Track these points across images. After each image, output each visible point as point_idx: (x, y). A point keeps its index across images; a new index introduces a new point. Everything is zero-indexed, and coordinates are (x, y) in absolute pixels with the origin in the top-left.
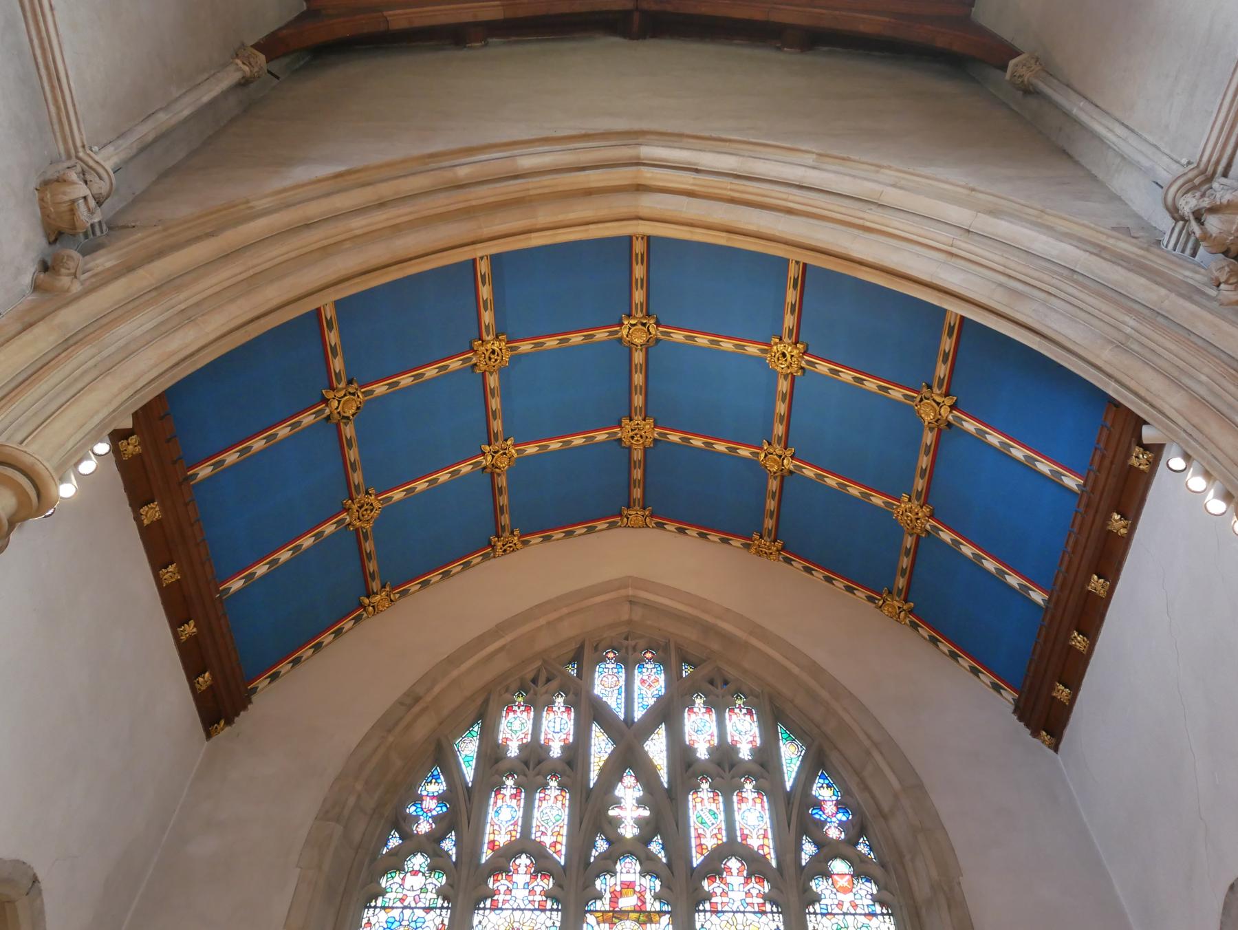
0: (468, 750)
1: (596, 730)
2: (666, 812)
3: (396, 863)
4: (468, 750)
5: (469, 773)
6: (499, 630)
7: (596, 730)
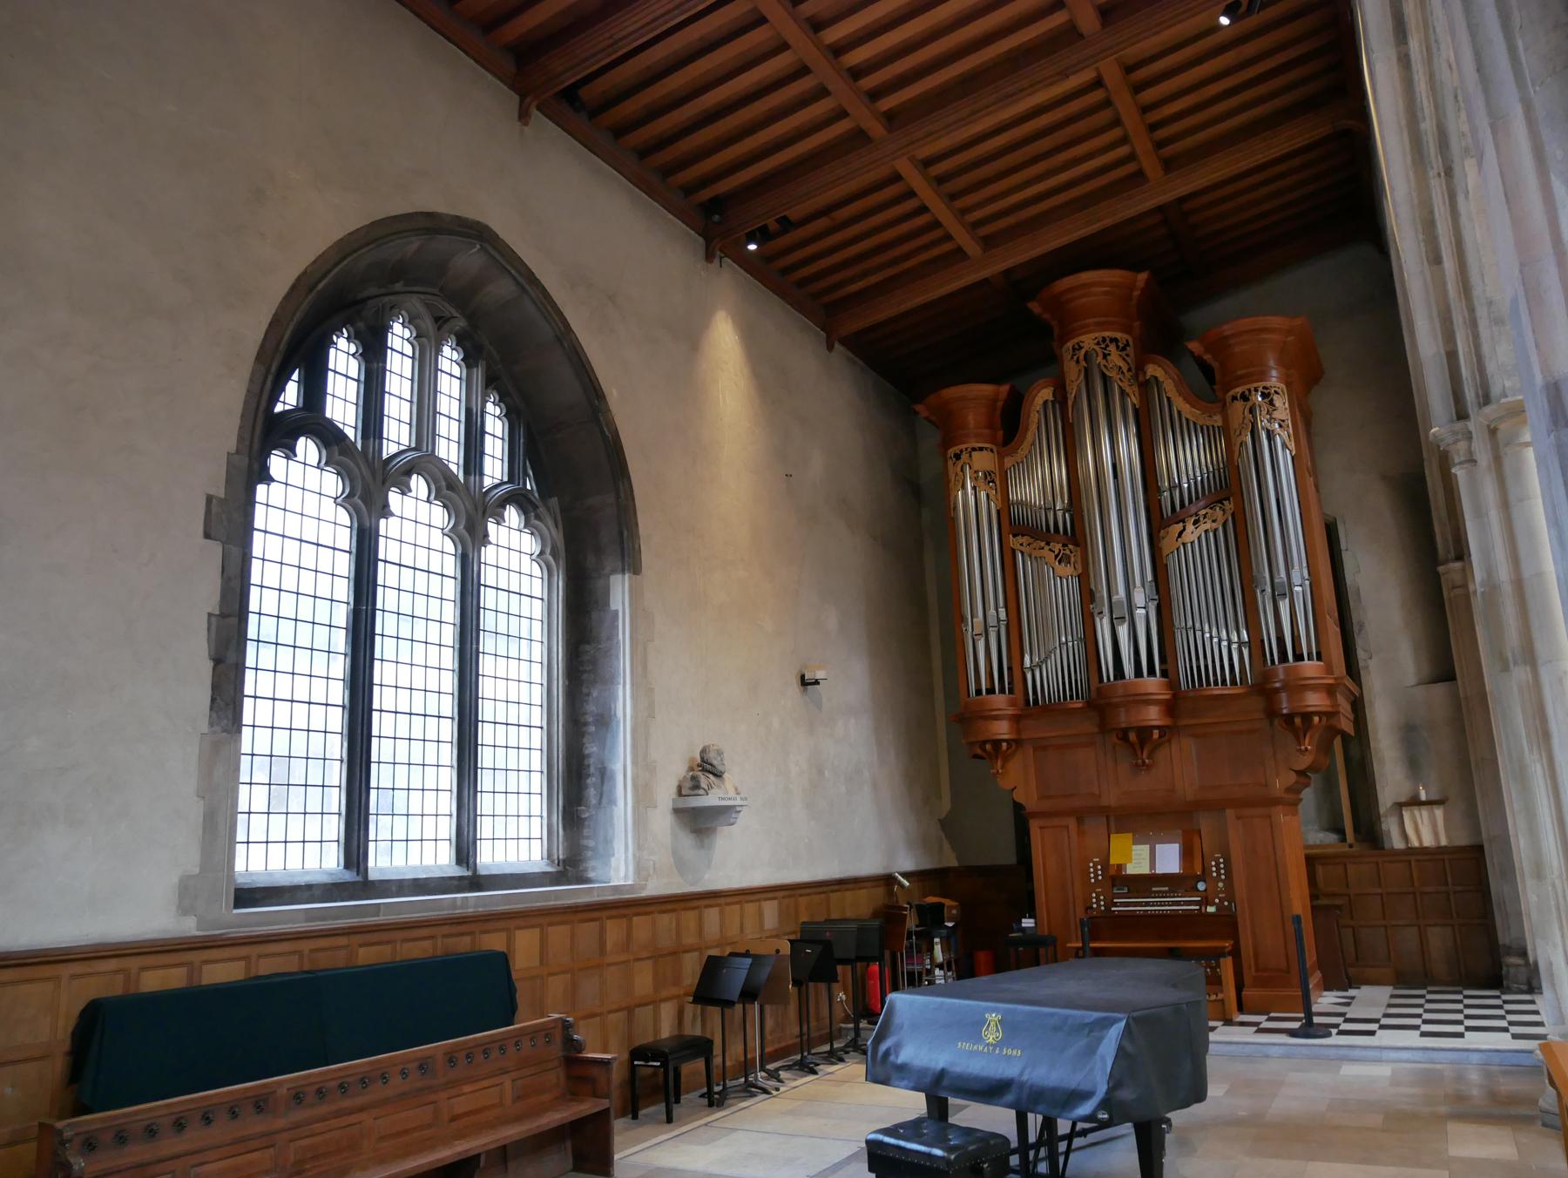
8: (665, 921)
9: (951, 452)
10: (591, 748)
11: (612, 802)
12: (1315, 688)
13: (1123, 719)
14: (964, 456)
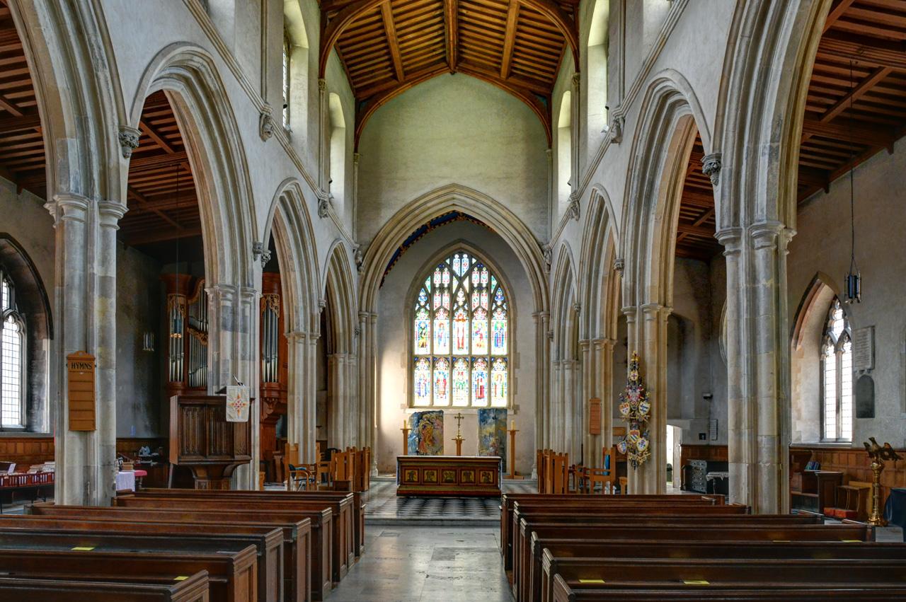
0: (428, 283)
1: (454, 278)
2: (468, 297)
3: (419, 310)
5: (429, 291)
7: (454, 278)
9: (169, 295)
10: (36, 393)
11: (42, 409)
12: (275, 390)
14: (174, 298)
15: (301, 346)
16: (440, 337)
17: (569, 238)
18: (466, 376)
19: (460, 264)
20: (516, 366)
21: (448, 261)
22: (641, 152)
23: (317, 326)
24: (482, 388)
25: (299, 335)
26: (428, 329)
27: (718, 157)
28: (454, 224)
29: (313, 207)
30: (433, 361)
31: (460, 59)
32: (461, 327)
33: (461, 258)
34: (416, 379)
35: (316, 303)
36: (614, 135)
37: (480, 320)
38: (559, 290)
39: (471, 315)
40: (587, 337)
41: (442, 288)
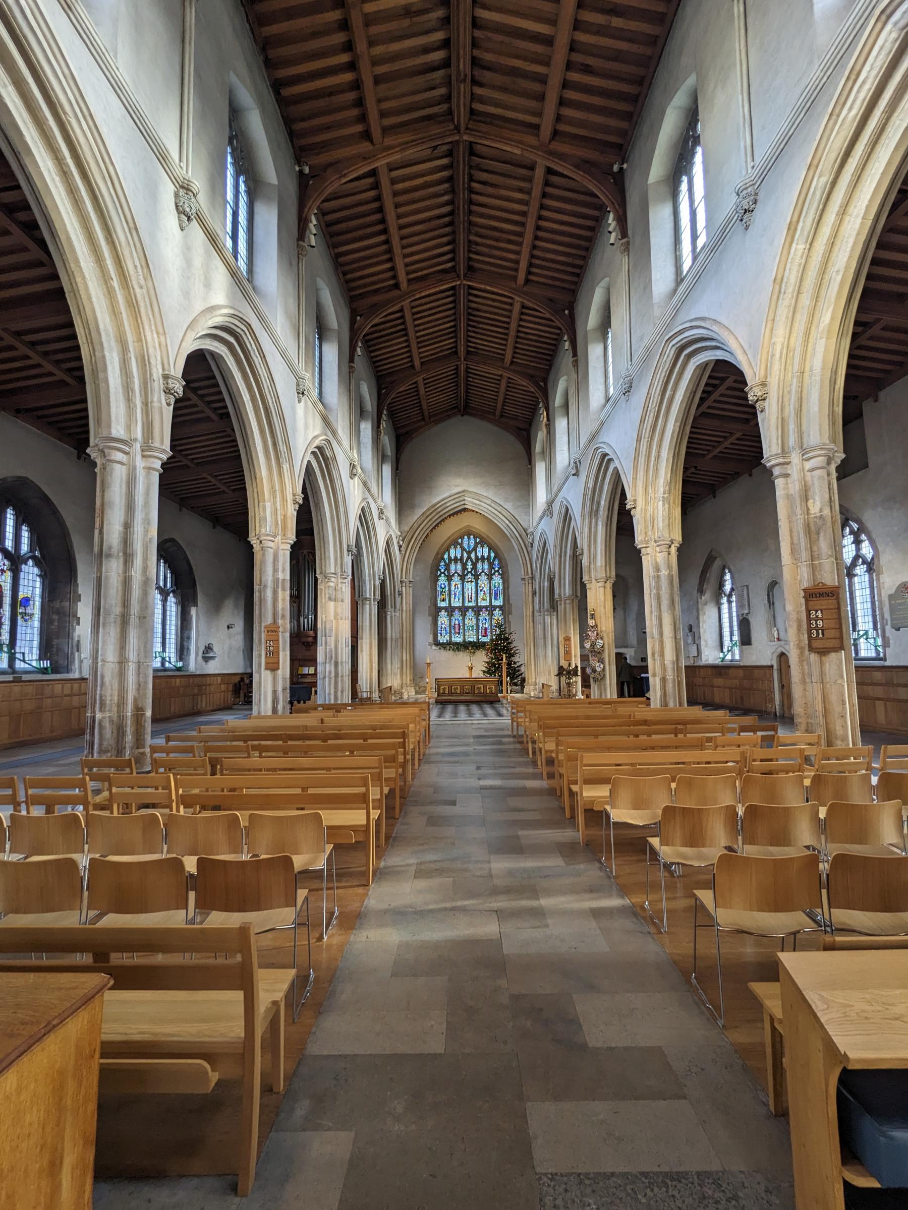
0: (446, 556)
2: (475, 565)
4: (446, 556)
6: (448, 539)
8: (200, 679)
10: (185, 644)
13: (304, 640)
15: (368, 606)
16: (455, 594)
17: (546, 529)
18: (474, 622)
19: (468, 543)
20: (510, 613)
21: (460, 541)
22: (591, 485)
23: (378, 593)
24: (486, 629)
25: (366, 599)
26: (447, 588)
27: (635, 501)
28: (465, 514)
29: (375, 514)
30: (450, 610)
31: (466, 406)
32: (470, 587)
33: (469, 538)
34: (439, 624)
35: (377, 577)
36: (574, 472)
37: (483, 580)
38: (539, 562)
39: (477, 577)
40: (560, 595)
41: (456, 559)
